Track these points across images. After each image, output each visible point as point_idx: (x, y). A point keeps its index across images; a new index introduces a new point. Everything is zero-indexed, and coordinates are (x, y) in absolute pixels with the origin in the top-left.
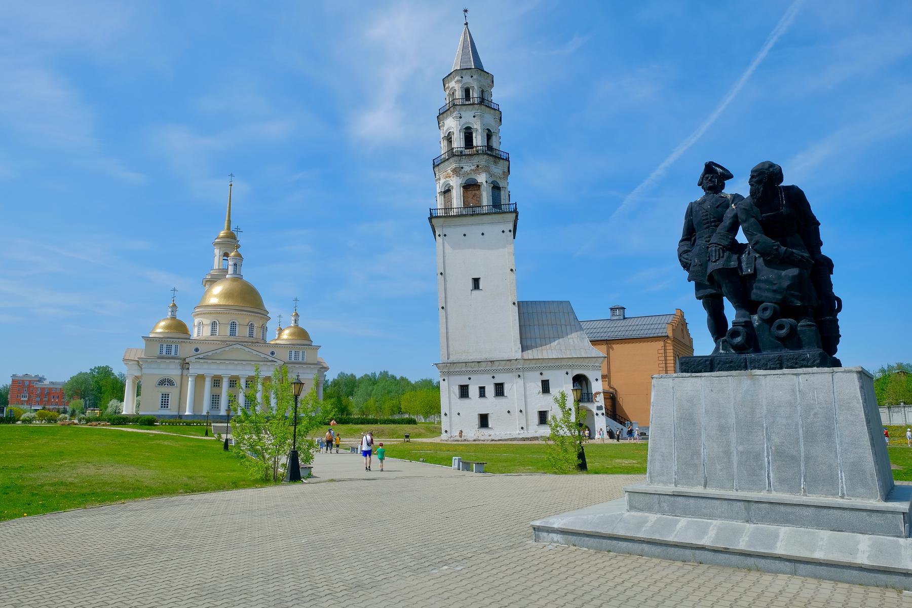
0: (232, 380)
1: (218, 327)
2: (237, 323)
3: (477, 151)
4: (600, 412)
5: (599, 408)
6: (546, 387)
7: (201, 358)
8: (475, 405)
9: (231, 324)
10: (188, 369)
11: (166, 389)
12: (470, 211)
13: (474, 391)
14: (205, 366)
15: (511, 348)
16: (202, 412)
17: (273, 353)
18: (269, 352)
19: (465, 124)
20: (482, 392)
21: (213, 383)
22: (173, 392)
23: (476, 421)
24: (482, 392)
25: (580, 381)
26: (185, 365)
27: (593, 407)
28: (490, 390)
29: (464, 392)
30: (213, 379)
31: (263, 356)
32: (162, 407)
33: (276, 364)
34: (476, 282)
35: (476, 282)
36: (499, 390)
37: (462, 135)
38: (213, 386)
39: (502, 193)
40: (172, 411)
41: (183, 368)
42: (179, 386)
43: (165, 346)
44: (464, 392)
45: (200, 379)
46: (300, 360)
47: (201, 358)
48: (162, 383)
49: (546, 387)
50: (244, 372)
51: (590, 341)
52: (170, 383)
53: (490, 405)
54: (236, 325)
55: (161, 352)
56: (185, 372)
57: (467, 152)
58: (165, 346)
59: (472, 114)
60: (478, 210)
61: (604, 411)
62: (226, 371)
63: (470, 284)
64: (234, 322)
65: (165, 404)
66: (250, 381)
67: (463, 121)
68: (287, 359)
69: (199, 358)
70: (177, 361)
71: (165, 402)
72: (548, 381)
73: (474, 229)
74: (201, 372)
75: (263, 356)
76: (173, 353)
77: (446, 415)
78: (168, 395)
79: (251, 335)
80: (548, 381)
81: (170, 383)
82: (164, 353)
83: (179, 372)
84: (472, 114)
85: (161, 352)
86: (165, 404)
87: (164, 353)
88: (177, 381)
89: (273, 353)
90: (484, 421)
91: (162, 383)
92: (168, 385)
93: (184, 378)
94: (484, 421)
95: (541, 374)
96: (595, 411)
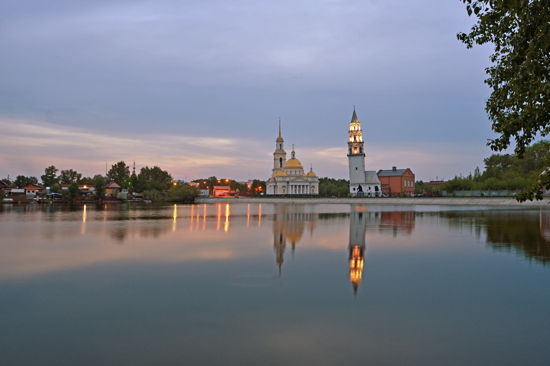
6: (370, 188)
11: (284, 188)
14: (293, 183)
18: (306, 179)
34: (357, 168)
35: (357, 168)
49: (370, 188)
50: (302, 184)
56: (288, 184)
62: (298, 184)
63: (355, 169)
65: (284, 192)
66: (303, 186)
79: (300, 174)
81: (285, 187)
83: (287, 184)
86: (284, 192)
88: (286, 187)
91: (283, 187)
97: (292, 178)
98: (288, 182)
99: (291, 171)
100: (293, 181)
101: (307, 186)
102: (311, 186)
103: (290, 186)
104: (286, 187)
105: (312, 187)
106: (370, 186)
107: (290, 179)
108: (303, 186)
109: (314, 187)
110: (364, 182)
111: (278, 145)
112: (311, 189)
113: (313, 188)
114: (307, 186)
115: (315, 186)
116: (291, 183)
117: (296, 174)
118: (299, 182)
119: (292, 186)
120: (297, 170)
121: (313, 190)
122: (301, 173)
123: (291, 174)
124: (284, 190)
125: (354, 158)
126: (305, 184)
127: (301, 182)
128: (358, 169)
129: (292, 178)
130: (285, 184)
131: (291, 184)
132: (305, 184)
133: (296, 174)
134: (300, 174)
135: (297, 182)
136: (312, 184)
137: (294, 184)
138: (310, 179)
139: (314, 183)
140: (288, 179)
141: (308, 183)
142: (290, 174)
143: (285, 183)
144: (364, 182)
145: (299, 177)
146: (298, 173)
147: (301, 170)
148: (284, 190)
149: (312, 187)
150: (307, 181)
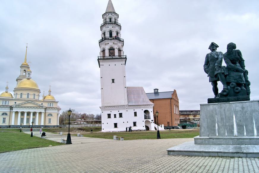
3: (114, 38)
4: (152, 122)
5: (152, 121)
6: (135, 114)
8: (113, 120)
10: (12, 109)
11: (4, 116)
12: (111, 57)
13: (112, 116)
14: (19, 109)
15: (124, 102)
16: (17, 124)
18: (40, 103)
19: (110, 29)
20: (115, 116)
22: (7, 118)
23: (113, 126)
24: (115, 116)
25: (146, 112)
26: (11, 108)
27: (150, 120)
28: (118, 116)
29: (109, 116)
31: (39, 105)
34: (113, 80)
35: (113, 80)
36: (121, 115)
37: (109, 33)
39: (121, 52)
40: (7, 124)
41: (11, 109)
42: (9, 115)
43: (4, 101)
44: (109, 116)
45: (17, 113)
46: (52, 106)
48: (3, 114)
49: (135, 114)
50: (32, 111)
51: (149, 100)
52: (6, 114)
53: (118, 120)
55: (3, 103)
56: (11, 110)
57: (110, 38)
58: (4, 101)
59: (112, 26)
60: (114, 57)
61: (154, 121)
62: (26, 110)
63: (111, 81)
65: (4, 121)
66: (34, 114)
67: (109, 28)
68: (47, 106)
69: (16, 106)
70: (8, 107)
72: (136, 112)
73: (112, 63)
74: (17, 111)
76: (7, 104)
77: (103, 124)
79: (34, 98)
80: (136, 112)
81: (6, 114)
82: (4, 104)
83: (9, 111)
84: (112, 26)
85: (3, 103)
86: (4, 121)
87: (4, 104)
88: (8, 114)
89: (42, 104)
90: (116, 125)
91: (3, 114)
93: (11, 112)
94: (116, 125)
95: (134, 110)
96: (151, 121)
97: (18, 103)
98: (11, 108)
99: (21, 94)
100: (18, 106)
101: (40, 113)
102: (47, 114)
103: (14, 114)
104: (8, 114)
105: (49, 115)
106: (135, 111)
107: (15, 103)
108: (34, 114)
109: (51, 115)
110: (127, 104)
111: (22, 70)
112: (47, 118)
113: (50, 117)
114: (40, 113)
115: (52, 114)
116: (16, 108)
117: (28, 97)
118: (28, 107)
119: (17, 113)
120: (31, 93)
121: (50, 119)
122: (36, 98)
123: (21, 97)
124: (4, 119)
125: (109, 63)
126: (38, 111)
127: (31, 107)
128: (115, 81)
129: (18, 103)
130: (7, 110)
131: (15, 110)
132: (38, 111)
133: (28, 97)
134: (34, 98)
135: (25, 107)
136: (48, 112)
137: (20, 110)
138: (46, 105)
139: (52, 110)
140: (11, 103)
141: (42, 109)
142: (20, 97)
143: (7, 109)
144: (127, 104)
145: (28, 101)
146: (31, 97)
147: (37, 94)
148: (4, 119)
149: (49, 115)
150: (41, 107)
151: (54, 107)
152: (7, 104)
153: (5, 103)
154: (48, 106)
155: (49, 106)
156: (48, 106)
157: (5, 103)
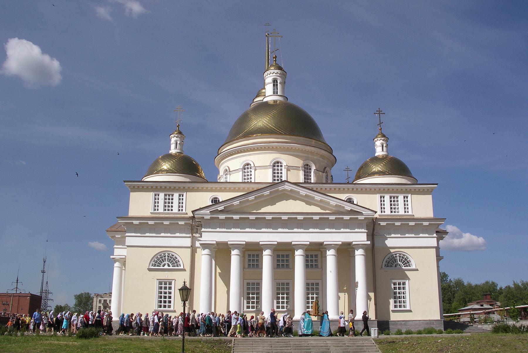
0: (281, 253)
1: (253, 171)
2: (284, 164)
7: (221, 212)
9: (274, 166)
17: (350, 201)
21: (247, 261)
30: (247, 253)
31: (333, 202)
32: (160, 306)
33: (360, 217)
38: (247, 266)
46: (401, 212)
47: (221, 212)
54: (281, 166)
64: (278, 162)
70: (181, 223)
71: (165, 297)
75: (333, 202)
78: (170, 283)
81: (174, 261)
83: (187, 242)
87: (161, 210)
88: (184, 257)
92: (169, 266)
151: (416, 216)
152: (175, 210)
153: (168, 204)
154: (382, 208)
155: (388, 212)
156: (382, 208)
157: (168, 204)
